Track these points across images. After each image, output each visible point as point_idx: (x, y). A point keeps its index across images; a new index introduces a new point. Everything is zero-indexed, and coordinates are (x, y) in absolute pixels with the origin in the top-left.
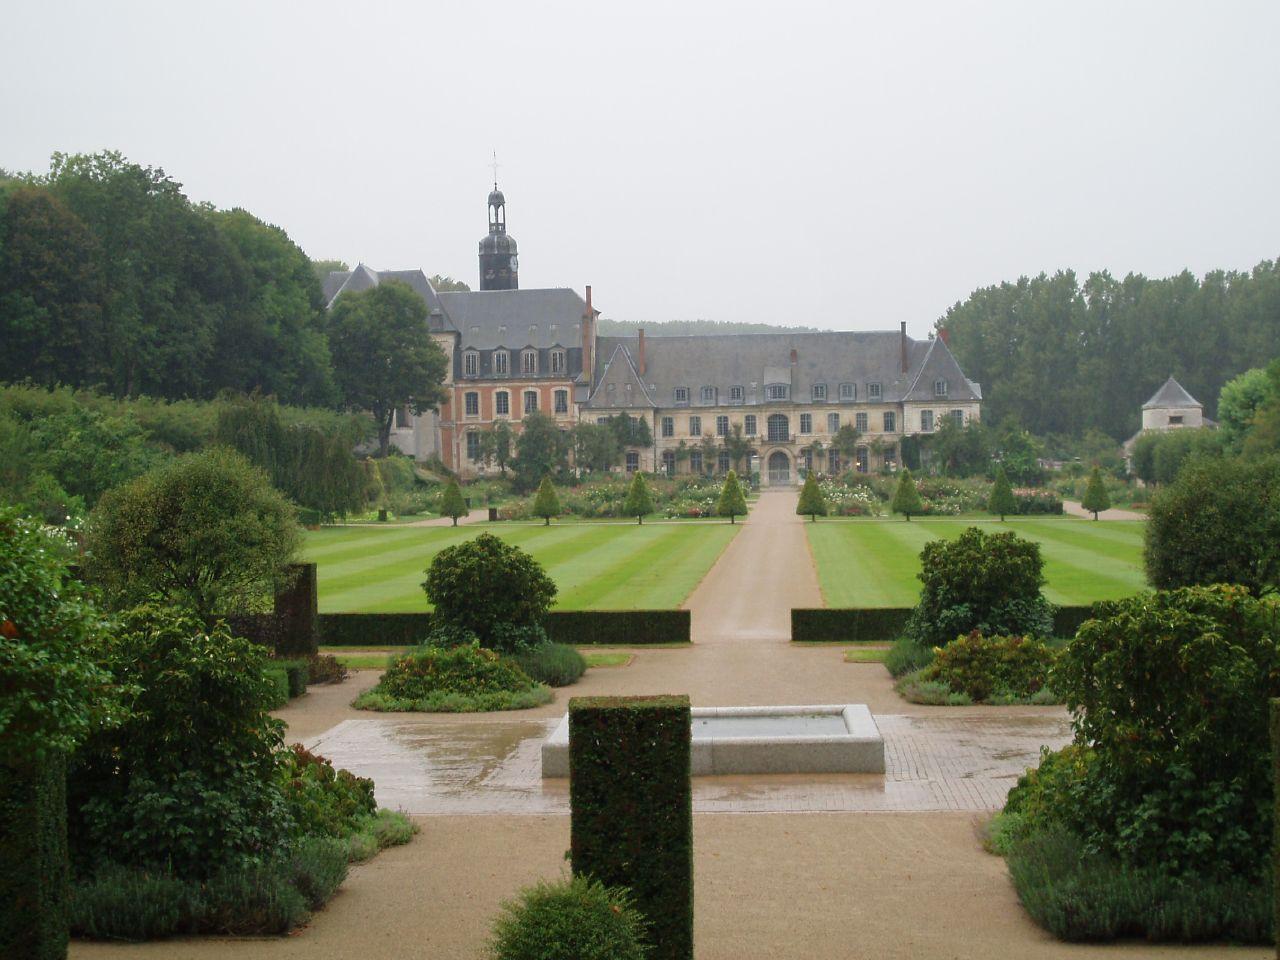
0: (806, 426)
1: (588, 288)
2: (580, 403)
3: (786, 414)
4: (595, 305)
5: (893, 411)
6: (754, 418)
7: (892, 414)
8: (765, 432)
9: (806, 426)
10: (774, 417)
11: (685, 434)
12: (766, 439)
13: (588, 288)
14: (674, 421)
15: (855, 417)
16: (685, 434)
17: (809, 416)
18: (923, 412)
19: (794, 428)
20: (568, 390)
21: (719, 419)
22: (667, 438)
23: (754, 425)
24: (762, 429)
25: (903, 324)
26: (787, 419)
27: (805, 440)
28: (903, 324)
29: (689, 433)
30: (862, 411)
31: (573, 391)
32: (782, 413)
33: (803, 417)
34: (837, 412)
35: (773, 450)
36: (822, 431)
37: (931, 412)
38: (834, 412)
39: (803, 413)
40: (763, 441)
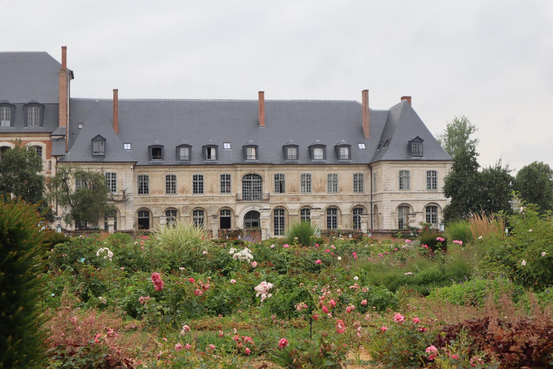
0: (280, 187)
1: (64, 49)
2: (56, 157)
3: (260, 173)
4: (69, 66)
5: (362, 172)
6: (228, 177)
7: (361, 175)
8: (240, 192)
9: (280, 187)
10: (248, 176)
11: (160, 192)
12: (241, 198)
13: (64, 49)
14: (150, 178)
15: (327, 176)
16: (160, 192)
17: (282, 176)
18: (401, 172)
19: (268, 187)
20: (44, 146)
21: (195, 177)
22: (141, 196)
23: (229, 184)
24: (237, 187)
25: (365, 93)
26: (261, 178)
27: (278, 199)
28: (365, 93)
29: (165, 190)
30: (333, 172)
31: (49, 148)
32: (257, 172)
33: (277, 177)
34: (309, 172)
35: (250, 209)
36: (294, 191)
37: (407, 172)
38: (306, 172)
39: (276, 173)
40: (238, 200)
